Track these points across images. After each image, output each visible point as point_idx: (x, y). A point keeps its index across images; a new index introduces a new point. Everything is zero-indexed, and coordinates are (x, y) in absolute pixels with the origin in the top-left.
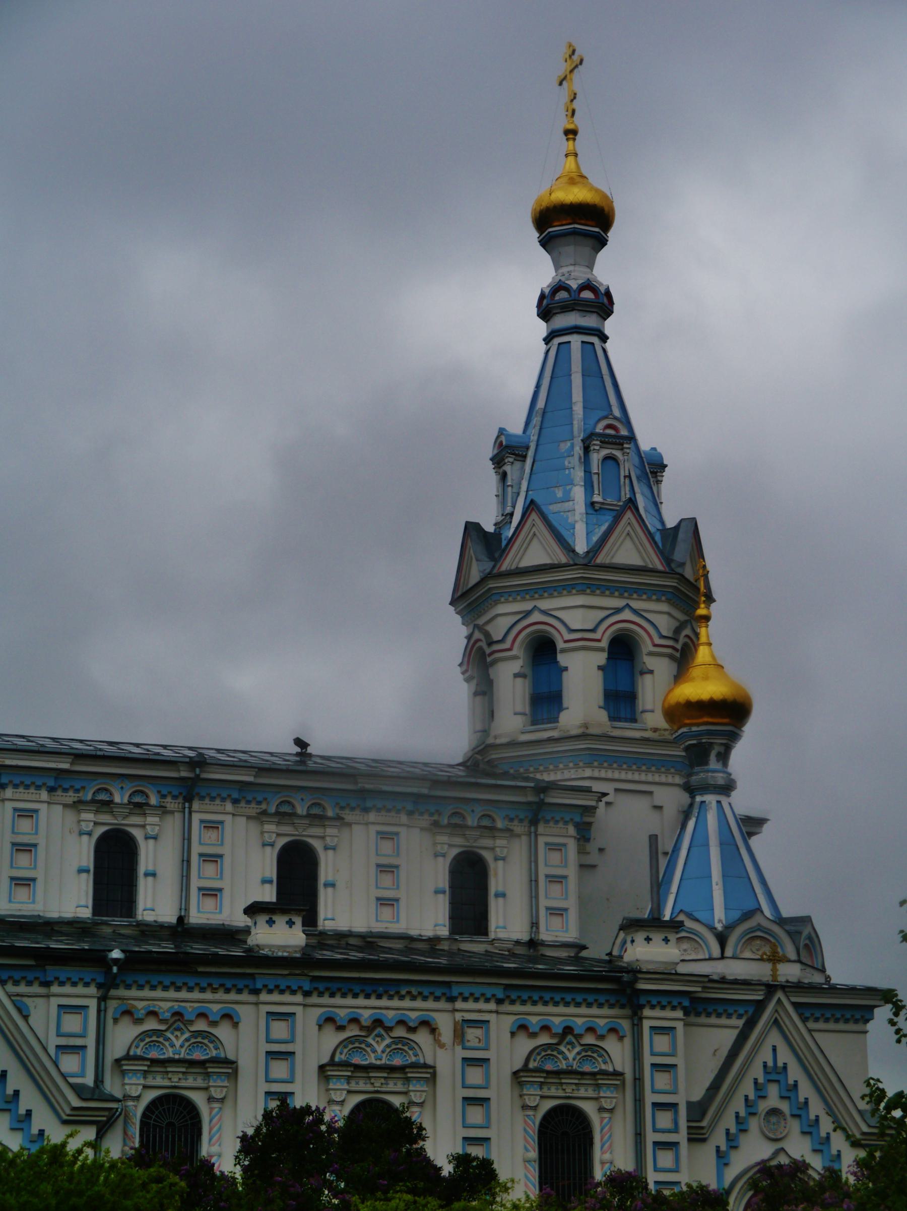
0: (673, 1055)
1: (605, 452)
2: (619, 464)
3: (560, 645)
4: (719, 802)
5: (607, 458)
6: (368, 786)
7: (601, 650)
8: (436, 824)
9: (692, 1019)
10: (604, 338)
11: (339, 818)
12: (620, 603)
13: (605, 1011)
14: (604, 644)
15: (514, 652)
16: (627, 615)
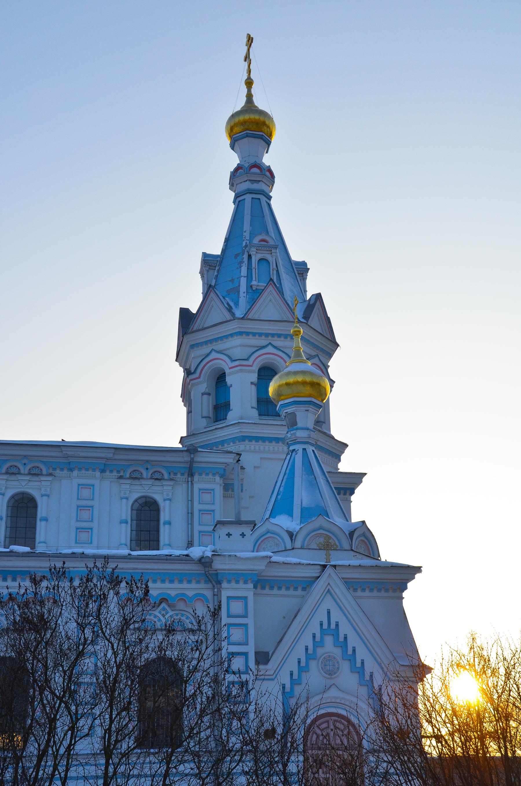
0: (245, 616)
1: (259, 256)
2: (269, 263)
3: (227, 371)
4: (304, 449)
5: (260, 260)
6: (69, 453)
7: (253, 372)
8: (121, 477)
9: (259, 591)
10: (270, 198)
11: (51, 475)
12: (265, 343)
13: (193, 585)
14: (256, 368)
15: (201, 379)
16: (270, 349)
